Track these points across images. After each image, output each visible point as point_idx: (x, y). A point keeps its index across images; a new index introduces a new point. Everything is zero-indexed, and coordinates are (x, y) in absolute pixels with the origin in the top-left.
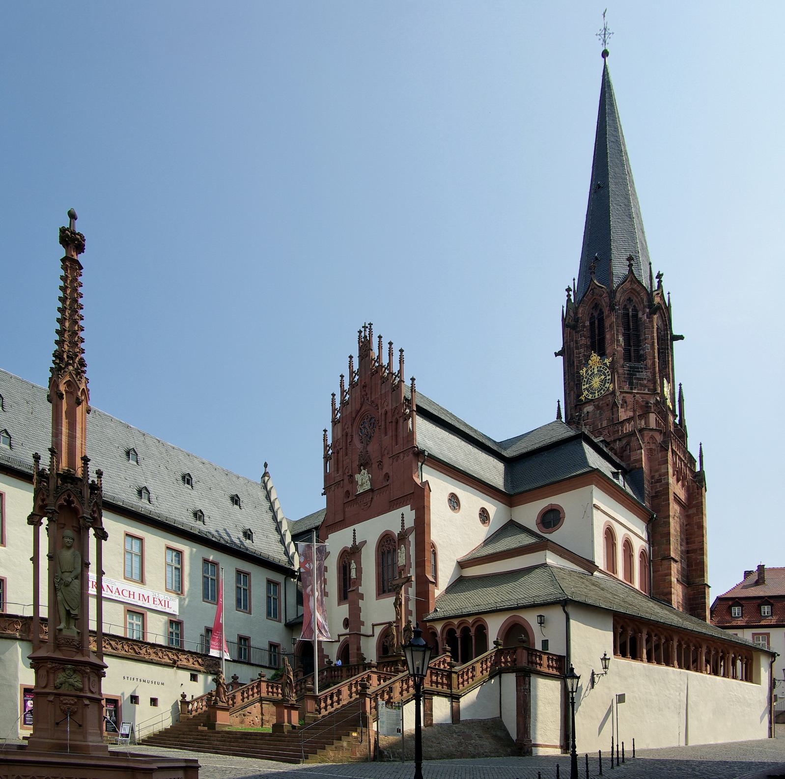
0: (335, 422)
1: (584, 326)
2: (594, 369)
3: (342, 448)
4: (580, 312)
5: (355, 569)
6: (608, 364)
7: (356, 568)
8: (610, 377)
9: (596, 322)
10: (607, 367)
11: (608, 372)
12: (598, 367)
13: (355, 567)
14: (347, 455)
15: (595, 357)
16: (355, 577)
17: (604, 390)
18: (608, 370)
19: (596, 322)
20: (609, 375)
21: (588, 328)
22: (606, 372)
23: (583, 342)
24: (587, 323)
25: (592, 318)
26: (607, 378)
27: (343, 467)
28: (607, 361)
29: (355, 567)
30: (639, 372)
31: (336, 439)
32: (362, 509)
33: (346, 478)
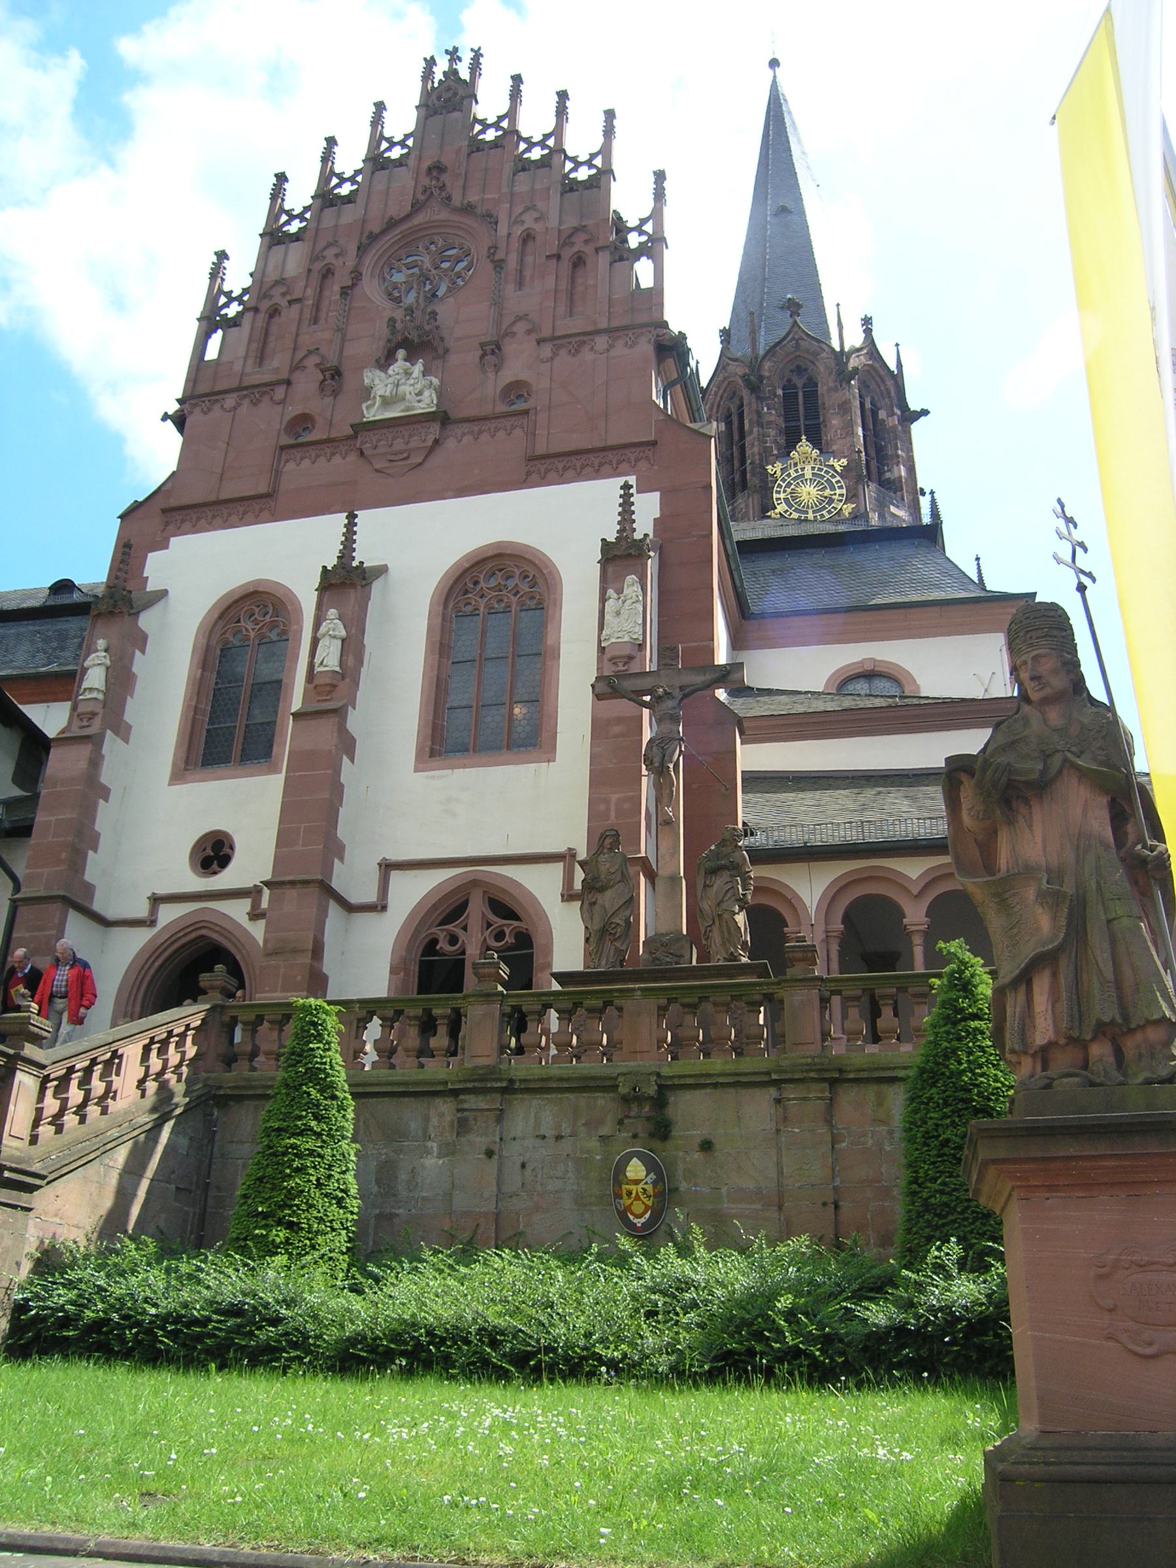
0: (273, 237)
1: (775, 395)
2: (803, 469)
3: (298, 300)
4: (766, 367)
5: (339, 642)
6: (838, 469)
7: (343, 640)
8: (844, 491)
9: (801, 394)
10: (836, 471)
11: (838, 482)
12: (813, 468)
13: (343, 633)
14: (315, 323)
15: (804, 446)
16: (338, 669)
17: (829, 512)
18: (838, 478)
19: (801, 394)
20: (840, 488)
21: (781, 400)
22: (834, 481)
23: (772, 418)
24: (780, 392)
25: (788, 386)
26: (838, 492)
27: (295, 349)
28: (839, 464)
29: (343, 633)
30: (893, 504)
31: (272, 276)
32: (377, 471)
33: (307, 383)
